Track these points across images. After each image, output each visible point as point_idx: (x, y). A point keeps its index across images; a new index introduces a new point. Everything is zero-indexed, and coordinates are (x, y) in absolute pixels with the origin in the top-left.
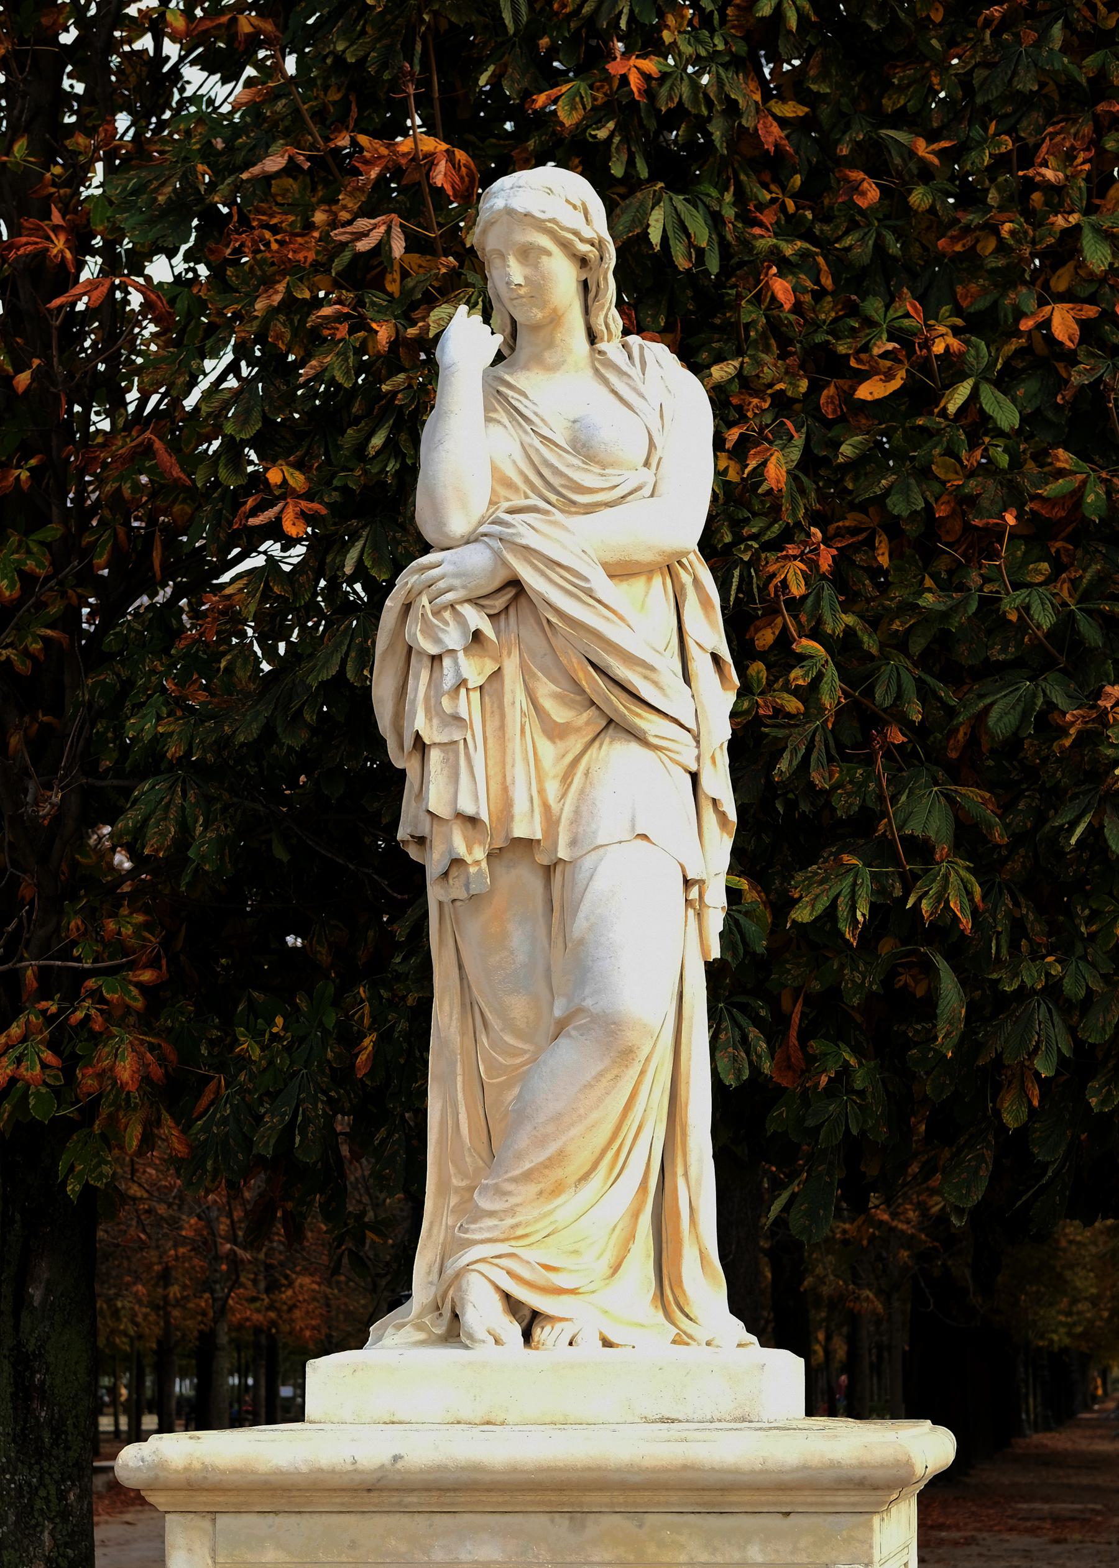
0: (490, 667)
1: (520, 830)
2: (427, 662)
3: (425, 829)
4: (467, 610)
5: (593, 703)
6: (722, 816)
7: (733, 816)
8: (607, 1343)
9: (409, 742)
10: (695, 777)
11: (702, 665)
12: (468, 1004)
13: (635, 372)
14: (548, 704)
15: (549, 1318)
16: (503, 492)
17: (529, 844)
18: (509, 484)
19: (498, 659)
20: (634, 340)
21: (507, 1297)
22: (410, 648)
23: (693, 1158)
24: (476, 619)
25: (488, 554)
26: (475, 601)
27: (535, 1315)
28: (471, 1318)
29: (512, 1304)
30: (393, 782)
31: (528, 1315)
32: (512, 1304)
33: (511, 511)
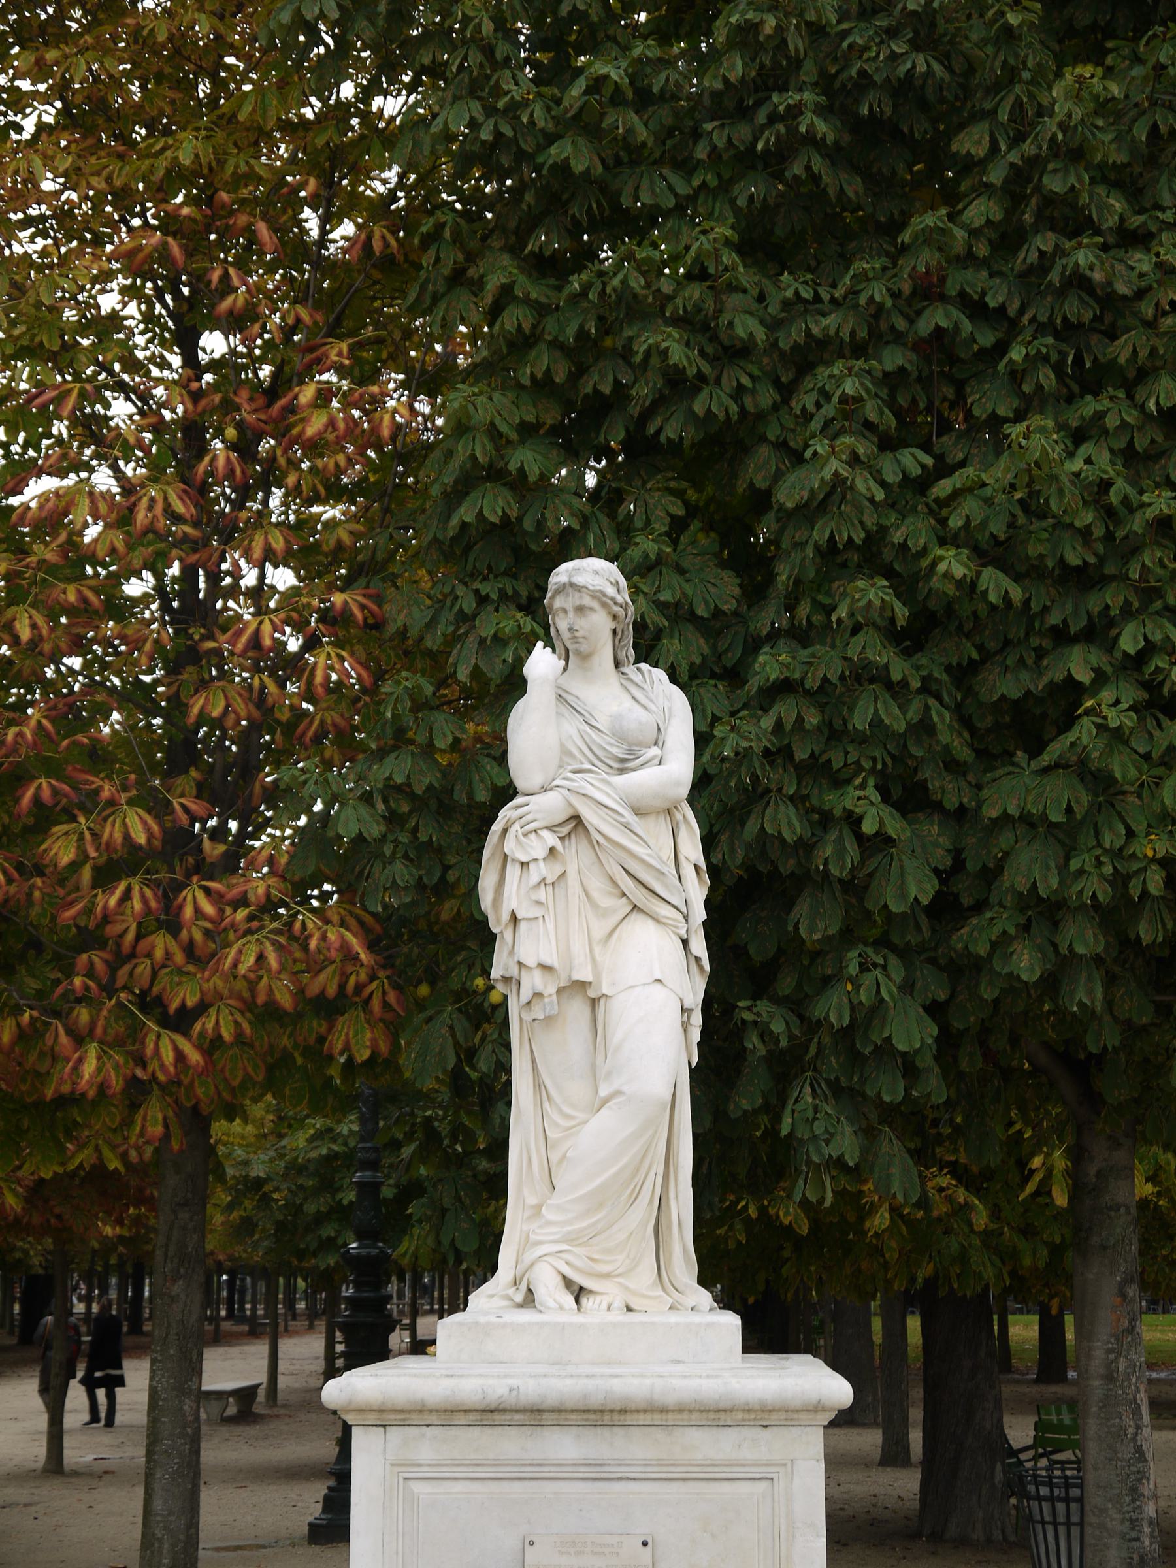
0: (558, 870)
1: (577, 976)
2: (518, 866)
3: (514, 971)
4: (546, 834)
5: (624, 895)
6: (701, 968)
7: (707, 968)
8: (629, 1309)
9: (506, 916)
10: (685, 943)
11: (689, 872)
12: (539, 1086)
13: (647, 687)
14: (595, 895)
15: (591, 1292)
16: (566, 759)
17: (582, 985)
18: (571, 754)
19: (564, 863)
20: (644, 666)
21: (564, 1277)
22: (506, 856)
23: (681, 1188)
24: (551, 839)
25: (560, 798)
26: (550, 828)
27: (581, 1289)
28: (540, 1293)
29: (568, 1283)
30: (488, 940)
31: (576, 1289)
32: (568, 1283)
33: (574, 772)
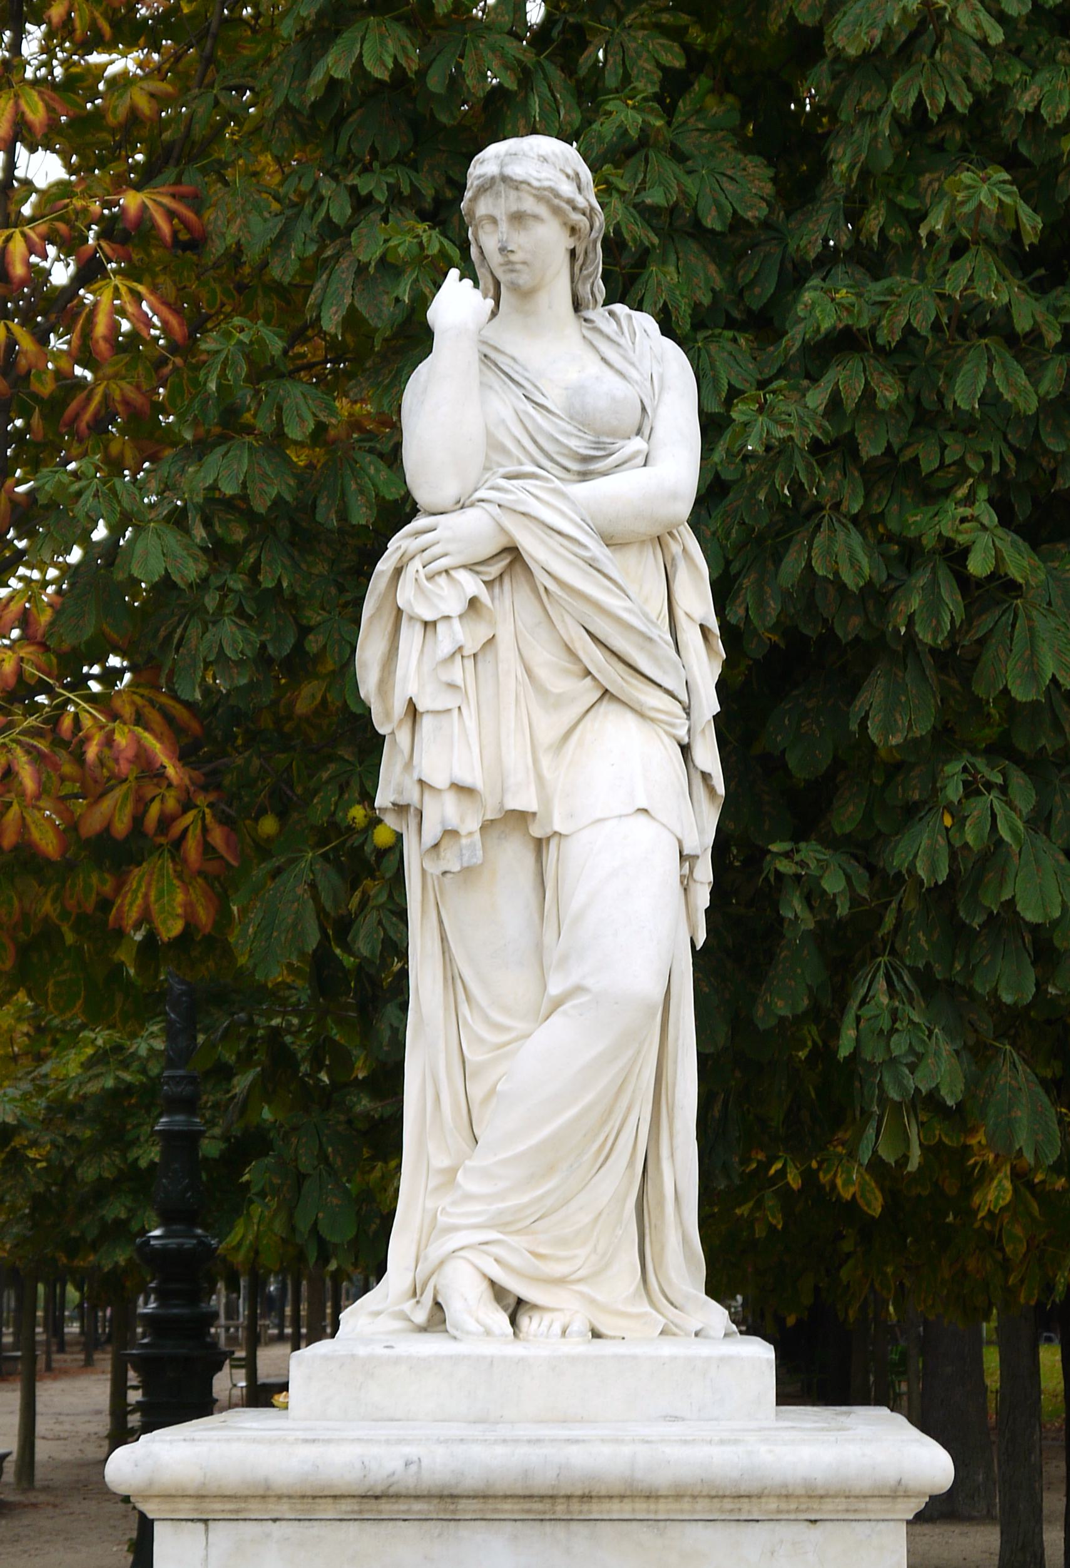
1: (512, 804)
2: (419, 628)
3: (412, 795)
4: (463, 576)
5: (588, 673)
6: (711, 790)
7: (721, 789)
8: (596, 1335)
9: (399, 707)
10: (686, 749)
11: (691, 637)
12: (452, 978)
15: (535, 1307)
16: (496, 457)
17: (521, 818)
18: (504, 450)
19: (492, 623)
20: (620, 308)
21: (492, 1283)
22: (399, 611)
23: (679, 1140)
24: (471, 585)
25: (486, 517)
26: (470, 567)
27: (520, 1302)
28: (454, 1310)
29: (499, 1292)
30: (371, 745)
31: (512, 1302)
32: (499, 1292)
33: (508, 477)
